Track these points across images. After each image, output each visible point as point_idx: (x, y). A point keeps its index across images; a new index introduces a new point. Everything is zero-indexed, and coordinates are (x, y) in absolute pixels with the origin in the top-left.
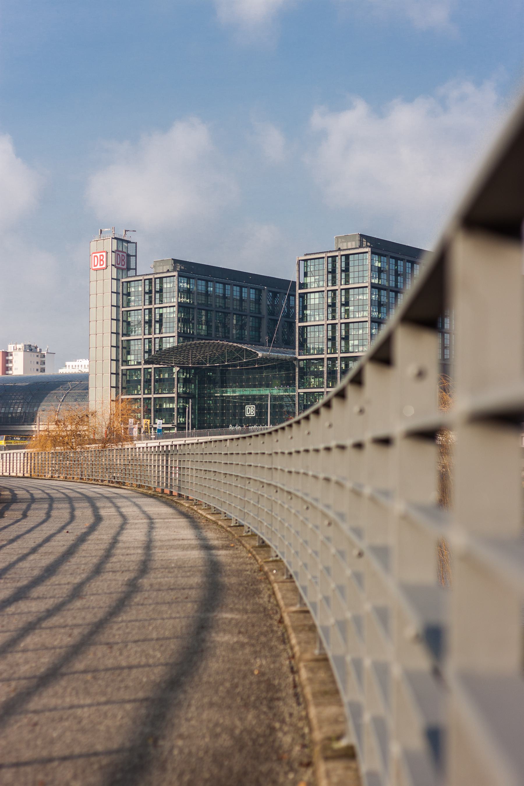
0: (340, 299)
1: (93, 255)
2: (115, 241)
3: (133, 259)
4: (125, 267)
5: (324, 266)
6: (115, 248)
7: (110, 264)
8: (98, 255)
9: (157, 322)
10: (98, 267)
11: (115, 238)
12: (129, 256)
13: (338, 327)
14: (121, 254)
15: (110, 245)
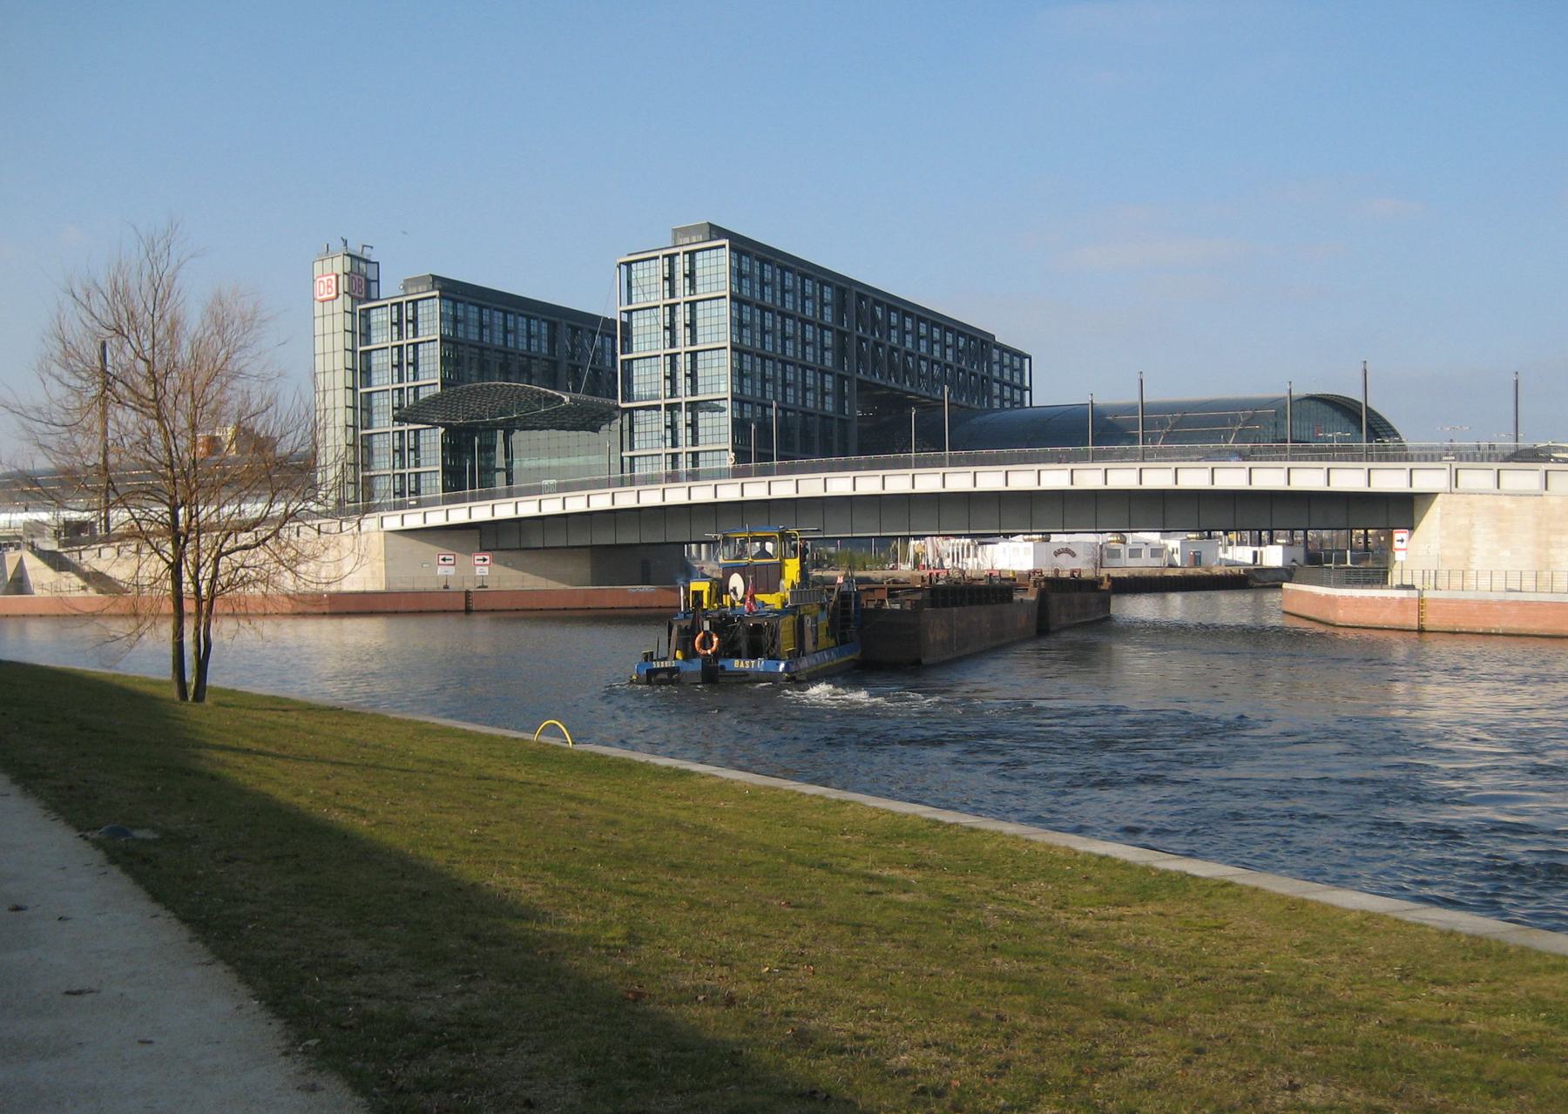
0: (682, 317)
1: (319, 280)
2: (348, 259)
3: (374, 285)
4: (363, 296)
5: (659, 268)
6: (348, 269)
7: (341, 291)
8: (325, 279)
9: (410, 321)
10: (326, 296)
11: (348, 255)
12: (368, 281)
13: (680, 359)
14: (357, 277)
15: (340, 265)
